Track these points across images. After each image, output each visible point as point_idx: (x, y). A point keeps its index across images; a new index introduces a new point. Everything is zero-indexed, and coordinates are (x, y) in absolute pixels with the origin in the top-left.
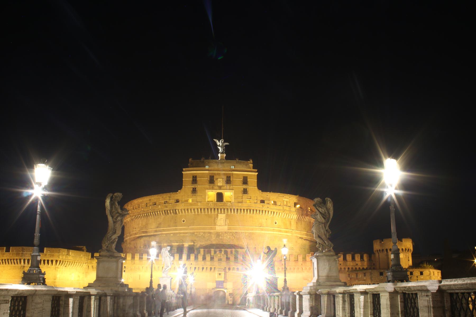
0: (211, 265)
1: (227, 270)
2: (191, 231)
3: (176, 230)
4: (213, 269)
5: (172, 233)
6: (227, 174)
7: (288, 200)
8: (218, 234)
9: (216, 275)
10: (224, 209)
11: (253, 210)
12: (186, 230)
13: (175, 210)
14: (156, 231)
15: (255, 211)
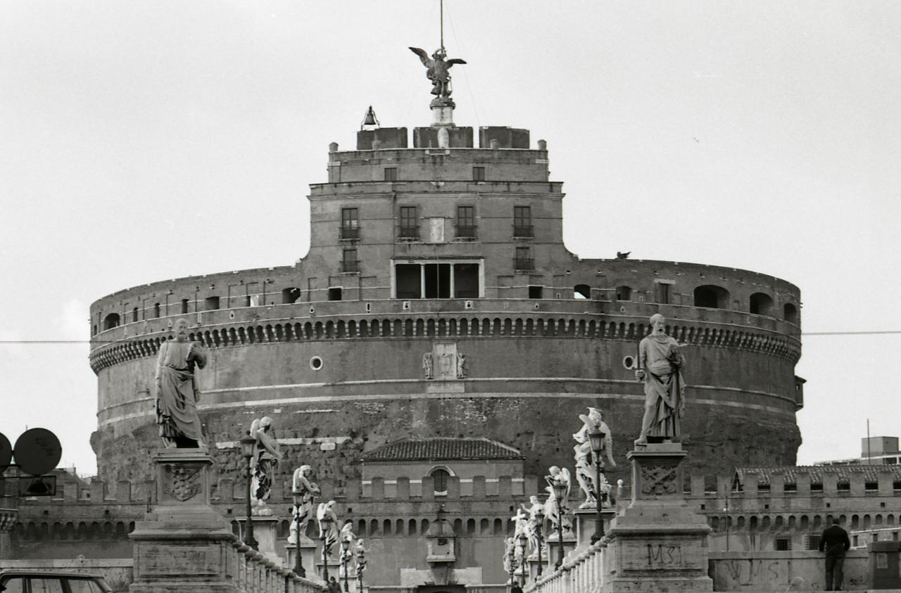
2: (344, 398)
4: (419, 526)
5: (278, 406)
7: (673, 282)
8: (434, 408)
13: (288, 326)
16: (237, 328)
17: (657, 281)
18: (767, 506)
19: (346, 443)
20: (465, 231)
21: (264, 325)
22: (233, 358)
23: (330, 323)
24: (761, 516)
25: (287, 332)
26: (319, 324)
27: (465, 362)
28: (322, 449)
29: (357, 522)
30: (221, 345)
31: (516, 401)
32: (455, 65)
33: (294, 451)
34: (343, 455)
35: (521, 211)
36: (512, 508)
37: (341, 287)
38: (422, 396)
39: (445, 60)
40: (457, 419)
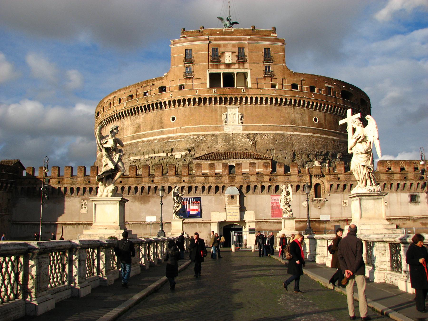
0: (217, 182)
1: (244, 190)
2: (186, 134)
3: (162, 133)
4: (220, 189)
5: (156, 140)
6: (238, 44)
7: (333, 87)
8: (227, 138)
9: (226, 199)
10: (236, 98)
11: (281, 99)
12: (177, 133)
13: (161, 103)
14: (133, 138)
15: (284, 100)
16: (139, 106)
17: (326, 85)
18: (405, 178)
19: (186, 155)
20: (241, 58)
21: (151, 103)
22: (138, 120)
23: (179, 101)
24: (402, 183)
25: (159, 106)
26: (174, 101)
27: (242, 117)
28: (176, 157)
29: (187, 188)
30: (134, 115)
31: (266, 135)
32: (234, 25)
33: (163, 159)
34: (185, 160)
35: (267, 51)
36: (270, 180)
37: (185, 84)
38: (222, 132)
39: (232, 22)
40: (238, 143)
